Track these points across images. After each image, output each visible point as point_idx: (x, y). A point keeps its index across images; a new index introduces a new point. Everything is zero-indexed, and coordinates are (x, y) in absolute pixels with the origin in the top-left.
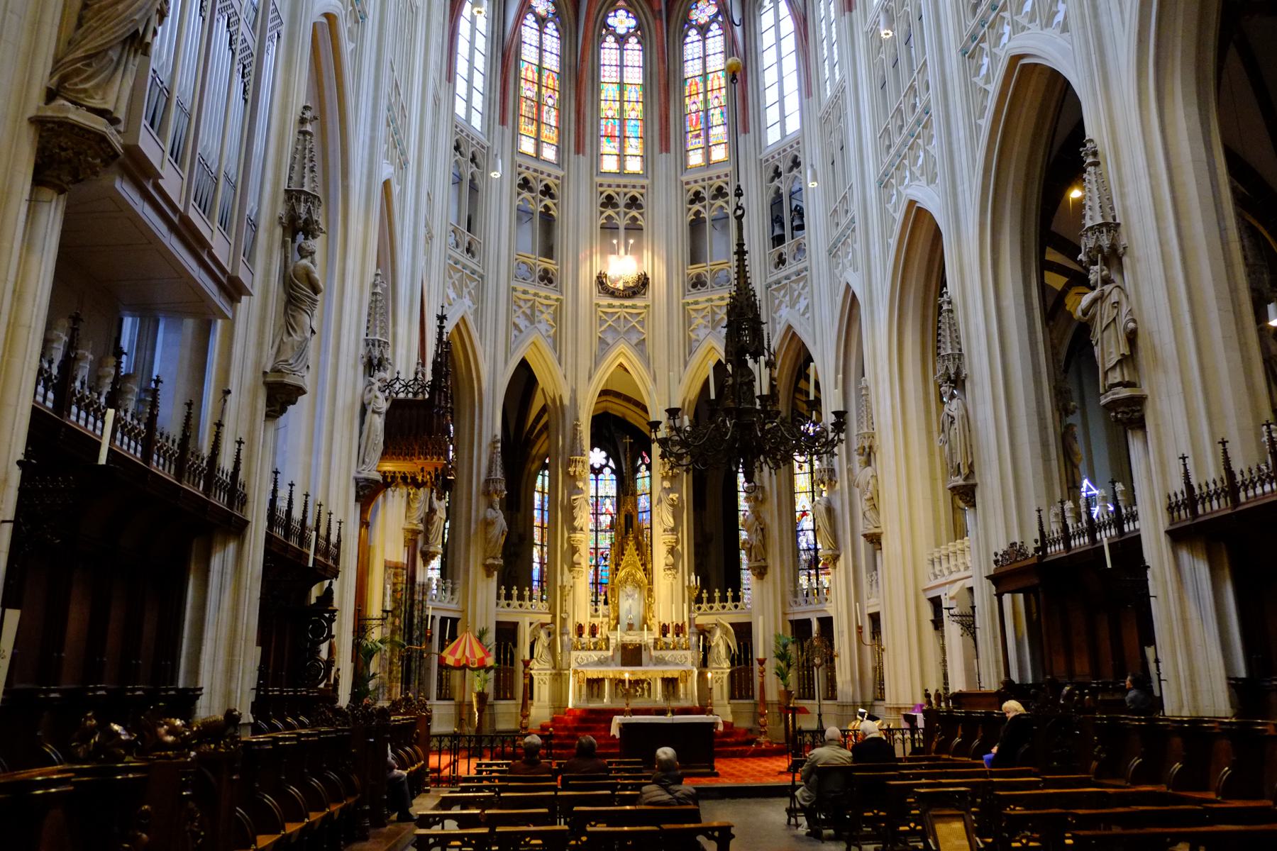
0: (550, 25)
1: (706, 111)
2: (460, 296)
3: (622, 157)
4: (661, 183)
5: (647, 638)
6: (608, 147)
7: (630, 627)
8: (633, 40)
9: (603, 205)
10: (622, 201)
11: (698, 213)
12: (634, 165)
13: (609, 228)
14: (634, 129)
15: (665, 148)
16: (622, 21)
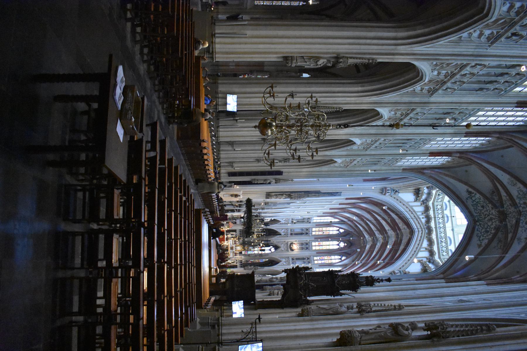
0: (338, 232)
1: (324, 260)
2: (284, 221)
3: (315, 246)
4: (310, 252)
5: (234, 250)
6: (317, 243)
7: (236, 248)
8: (338, 247)
9: (306, 243)
10: (307, 246)
11: (305, 259)
12: (314, 248)
13: (302, 244)
14: (321, 248)
15: (317, 253)
16: (342, 245)
